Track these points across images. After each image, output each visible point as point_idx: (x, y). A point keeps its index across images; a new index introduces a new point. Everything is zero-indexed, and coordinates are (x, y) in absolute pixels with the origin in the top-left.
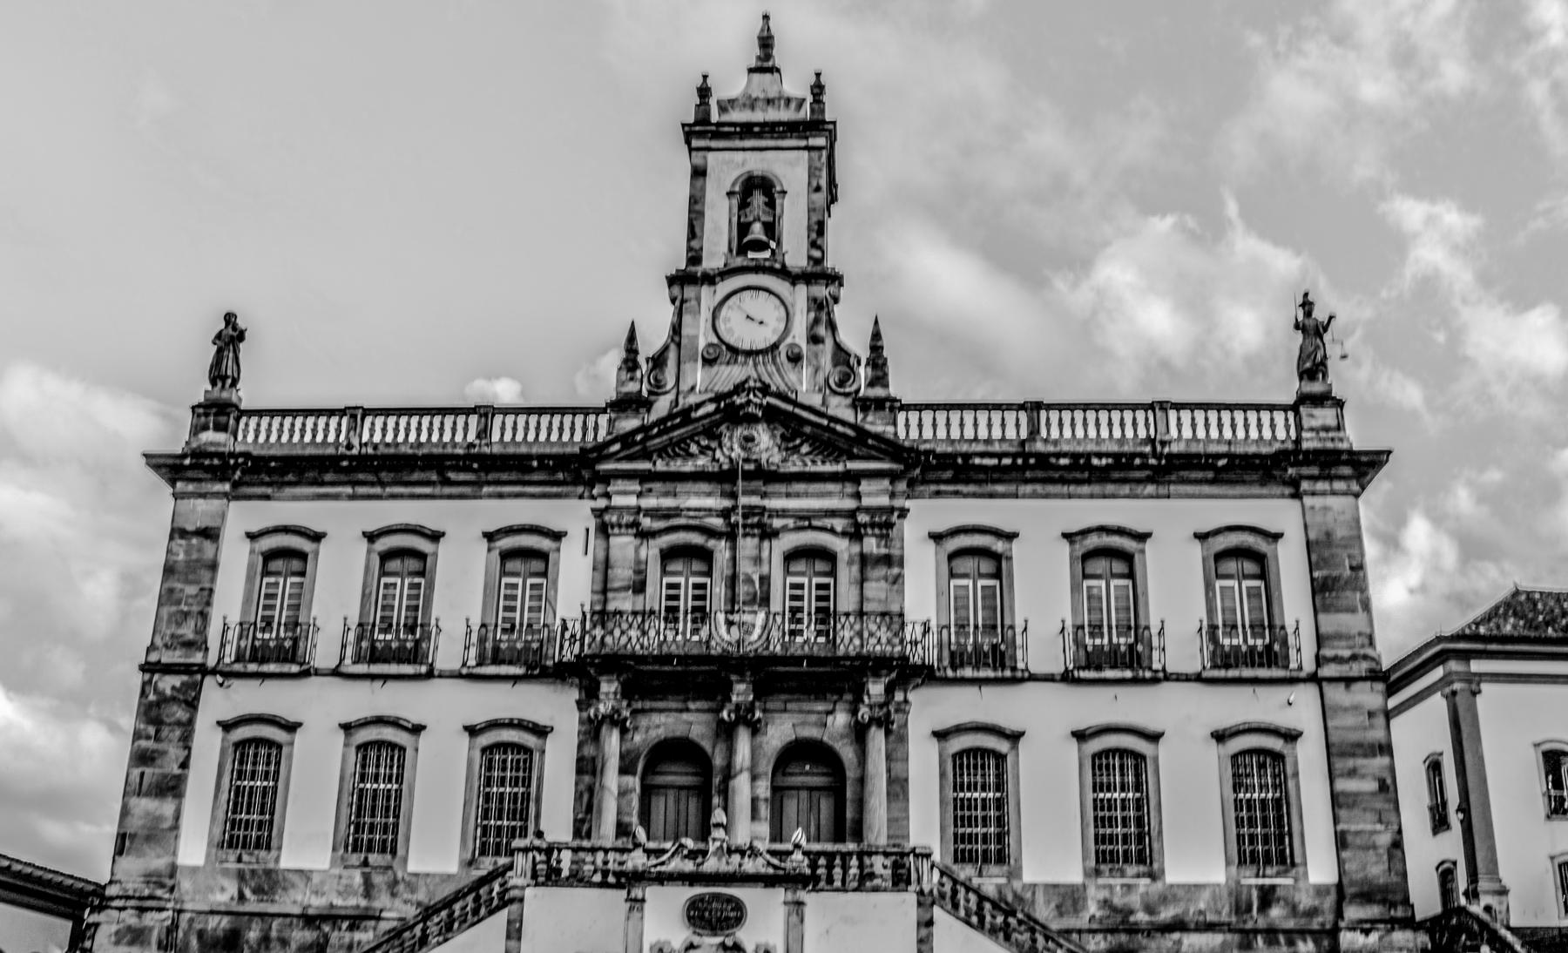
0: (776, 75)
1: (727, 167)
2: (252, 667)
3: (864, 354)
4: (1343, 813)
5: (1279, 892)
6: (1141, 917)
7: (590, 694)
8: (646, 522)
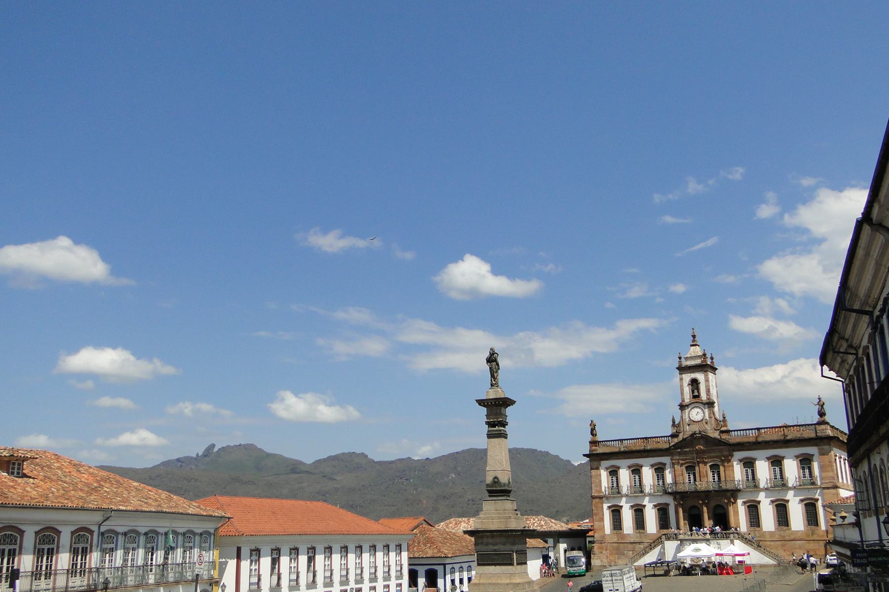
0: (697, 347)
1: (687, 377)
2: (612, 496)
3: (722, 419)
5: (816, 532)
6: (787, 537)
7: (675, 499)
8: (681, 462)
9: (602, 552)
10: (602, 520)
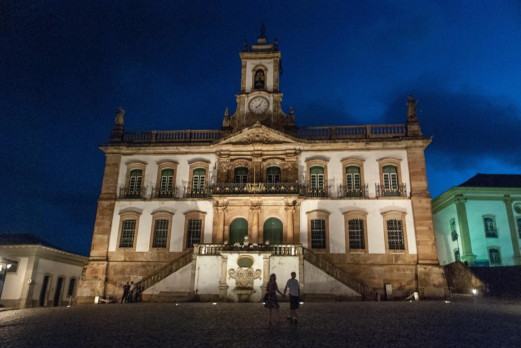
4: (418, 236)
5: (400, 257)
9: (96, 277)
10: (108, 232)
